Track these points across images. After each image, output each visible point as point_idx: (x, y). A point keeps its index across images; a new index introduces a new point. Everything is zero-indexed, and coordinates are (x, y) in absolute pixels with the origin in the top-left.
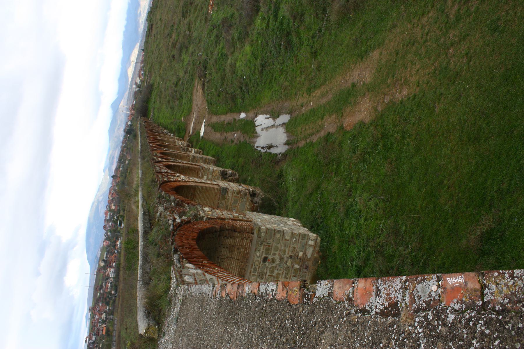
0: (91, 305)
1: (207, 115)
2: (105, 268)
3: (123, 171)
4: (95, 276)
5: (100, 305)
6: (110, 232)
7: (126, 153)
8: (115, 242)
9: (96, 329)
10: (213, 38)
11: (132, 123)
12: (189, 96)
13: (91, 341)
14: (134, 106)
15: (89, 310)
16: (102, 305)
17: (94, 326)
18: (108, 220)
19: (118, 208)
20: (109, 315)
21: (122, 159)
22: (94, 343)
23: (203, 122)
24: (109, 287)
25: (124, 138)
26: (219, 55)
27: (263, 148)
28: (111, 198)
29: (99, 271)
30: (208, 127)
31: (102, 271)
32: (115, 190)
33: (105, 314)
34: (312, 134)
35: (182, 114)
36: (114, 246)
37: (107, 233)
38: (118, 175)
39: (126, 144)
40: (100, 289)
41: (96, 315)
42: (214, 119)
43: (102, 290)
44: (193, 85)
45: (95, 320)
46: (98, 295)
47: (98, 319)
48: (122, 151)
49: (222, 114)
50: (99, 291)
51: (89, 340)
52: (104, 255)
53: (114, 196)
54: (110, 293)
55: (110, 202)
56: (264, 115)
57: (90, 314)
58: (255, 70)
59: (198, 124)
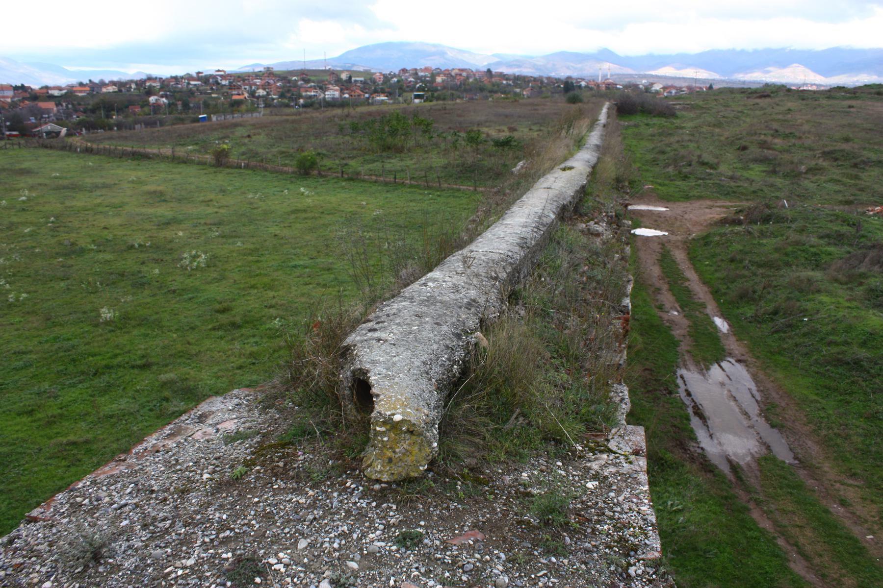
0: (276, 69)
1: (679, 238)
2: (338, 81)
4: (324, 68)
5: (278, 84)
6: (398, 81)
7: (532, 87)
8: (383, 92)
9: (239, 84)
10: (836, 227)
12: (695, 193)
13: (219, 78)
15: (268, 68)
16: (278, 87)
17: (244, 80)
18: (416, 74)
19: (439, 88)
20: (264, 101)
21: (520, 81)
22: (218, 83)
23: (661, 230)
24: (309, 93)
25: (556, 79)
26: (812, 250)
27: (689, 394)
28: (453, 73)
29: (332, 73)
30: (659, 244)
31: (332, 79)
32: (468, 77)
33: (265, 93)
34: (806, 557)
35: (657, 183)
36: (376, 92)
37: (395, 76)
38: (493, 80)
39: (548, 84)
40: (303, 80)
41: (261, 79)
42: (679, 256)
43: (302, 82)
44: (719, 198)
45: (253, 80)
46: (294, 78)
47: (255, 84)
48: (535, 80)
49: (697, 270)
50: (299, 78)
51: (221, 76)
52: (358, 77)
53: (458, 77)
54: (300, 97)
55: (447, 72)
56: (753, 384)
57: (262, 69)
58: (836, 344)
59: (655, 221)
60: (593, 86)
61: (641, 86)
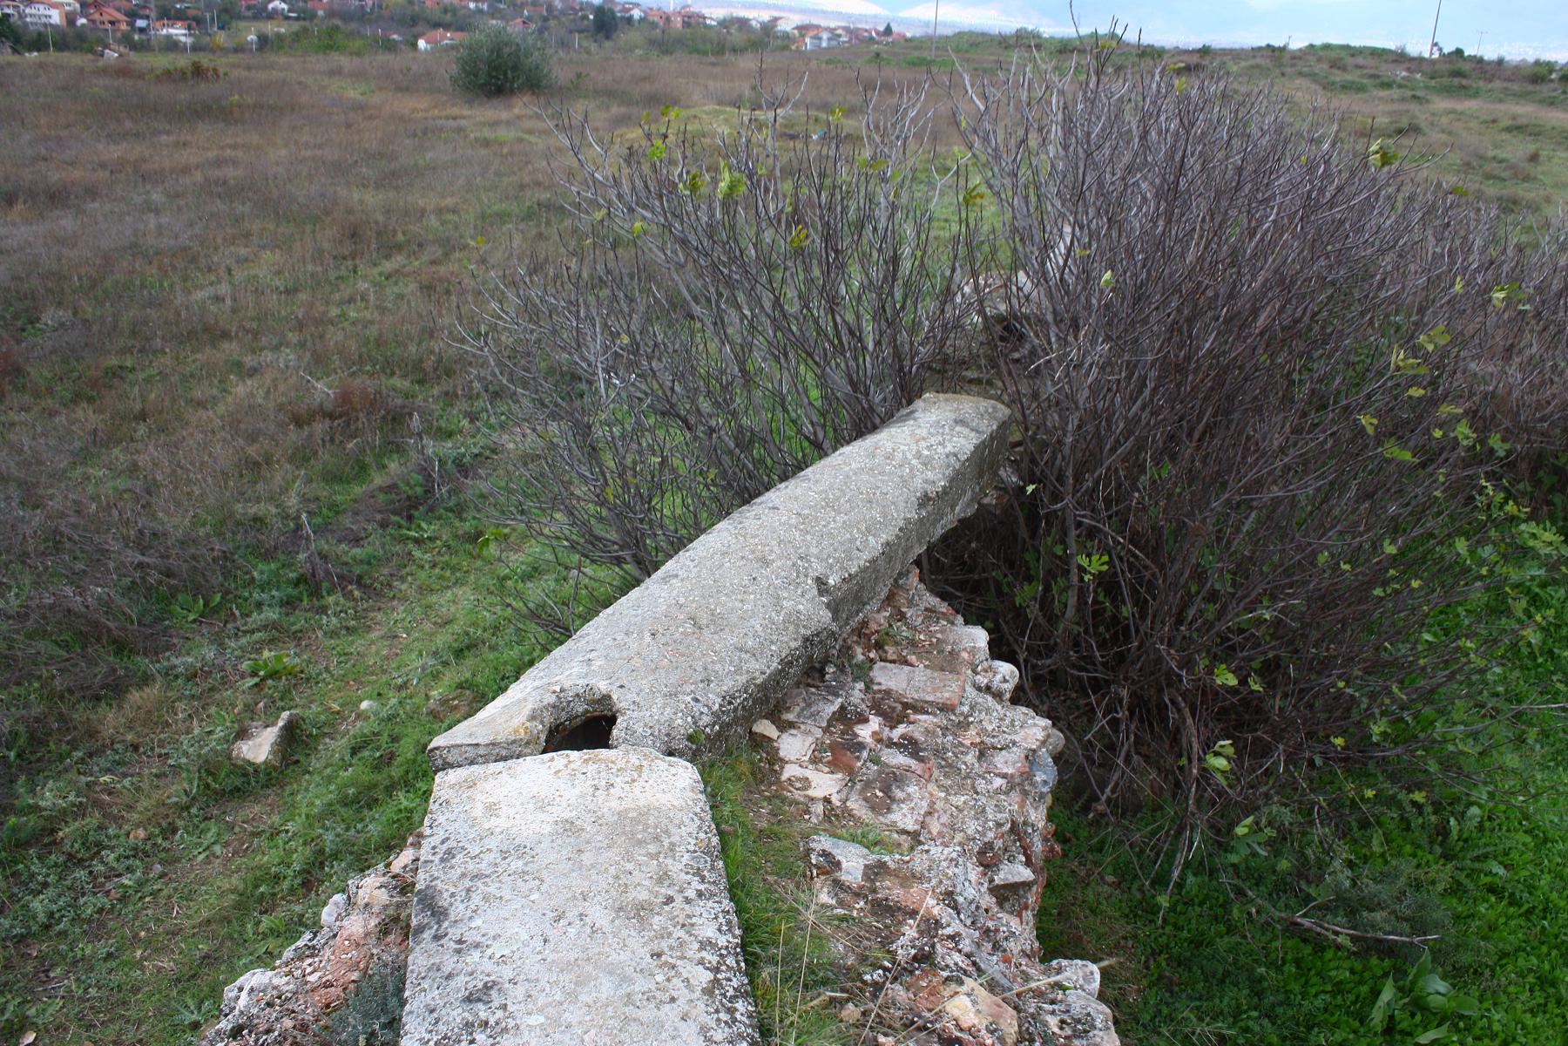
3: (462, 12)
11: (636, 24)
14: (699, 24)
39: (563, 12)
60: (656, 19)
61: (754, 23)
